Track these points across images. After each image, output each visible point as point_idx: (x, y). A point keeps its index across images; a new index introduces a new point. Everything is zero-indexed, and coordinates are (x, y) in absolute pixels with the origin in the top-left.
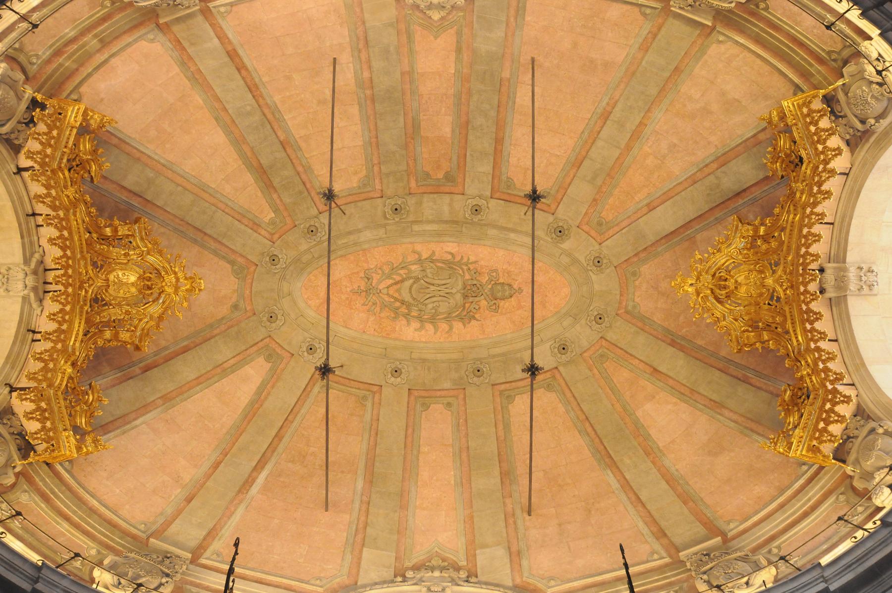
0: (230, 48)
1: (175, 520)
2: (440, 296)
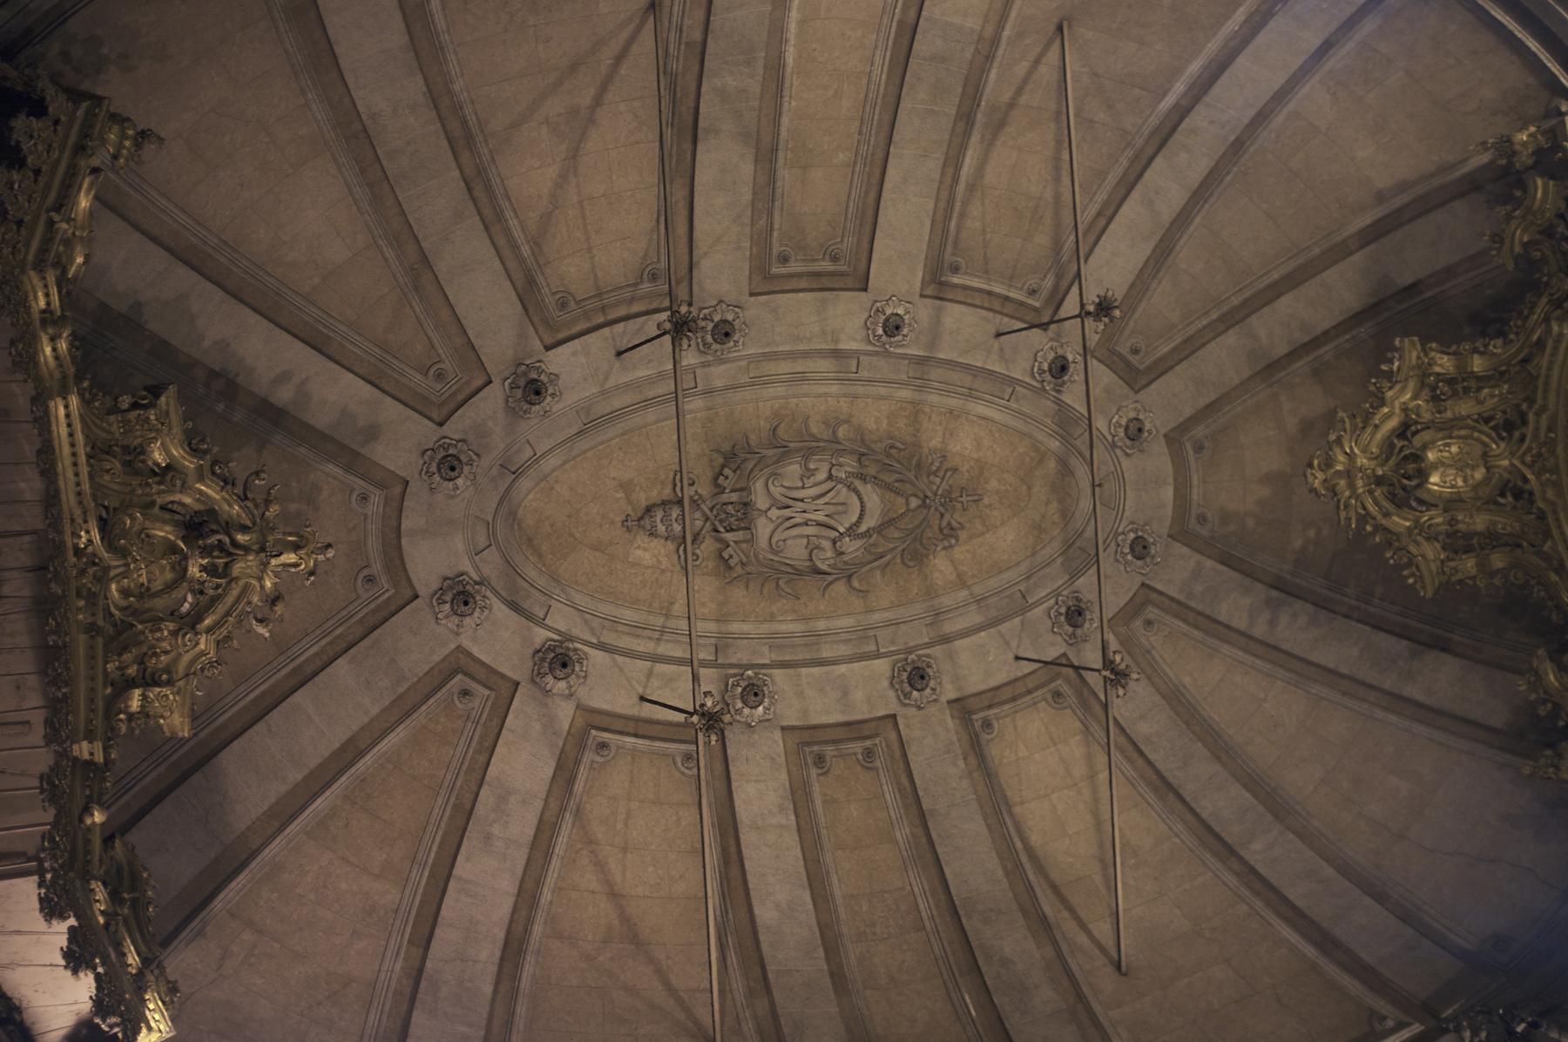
2: (802, 500)
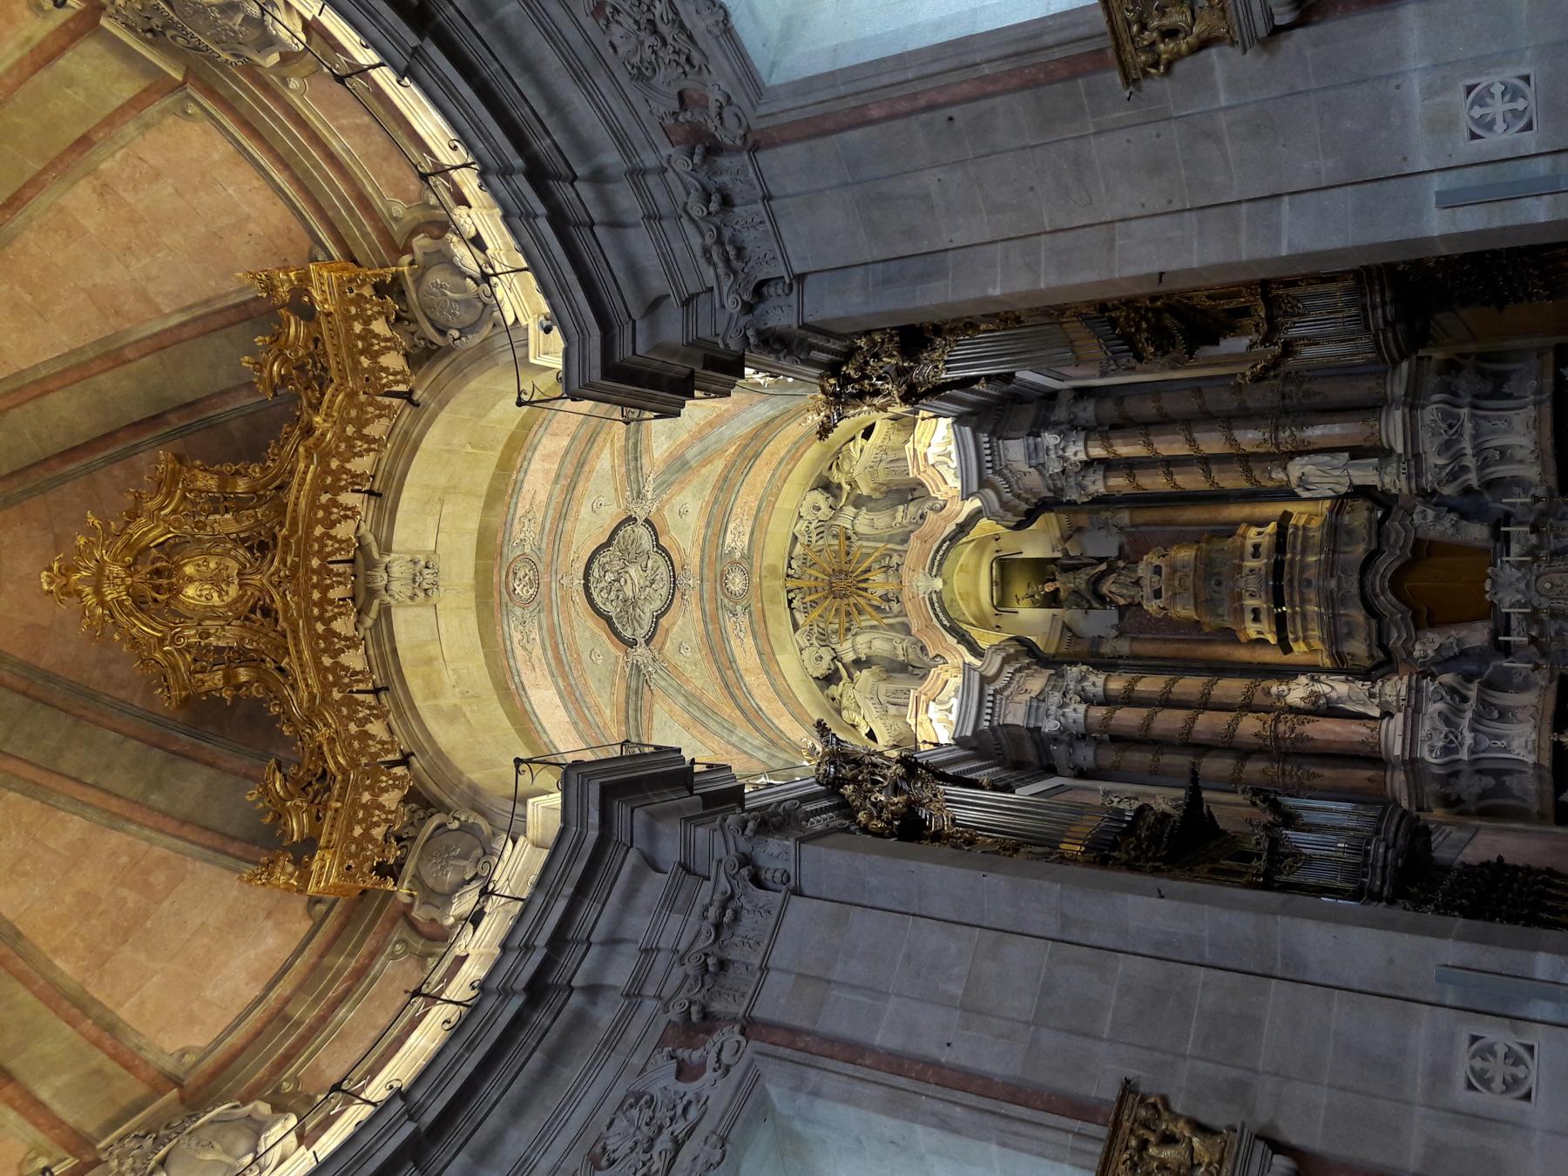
0: (9, 1090)
1: (122, 107)
